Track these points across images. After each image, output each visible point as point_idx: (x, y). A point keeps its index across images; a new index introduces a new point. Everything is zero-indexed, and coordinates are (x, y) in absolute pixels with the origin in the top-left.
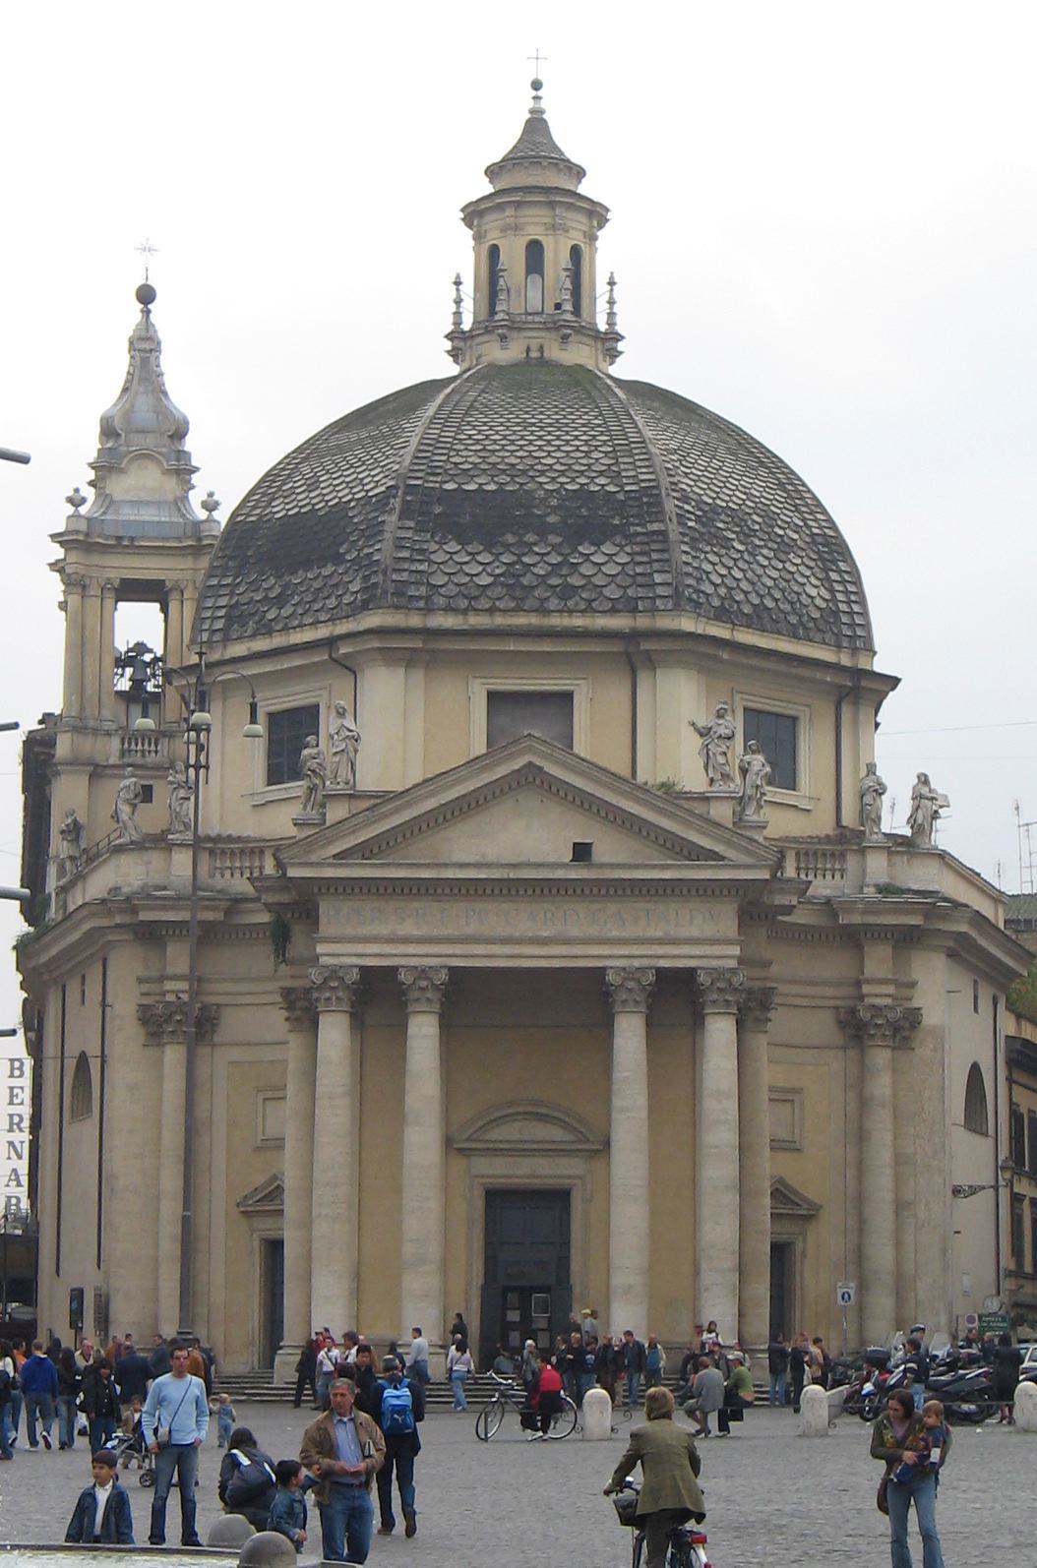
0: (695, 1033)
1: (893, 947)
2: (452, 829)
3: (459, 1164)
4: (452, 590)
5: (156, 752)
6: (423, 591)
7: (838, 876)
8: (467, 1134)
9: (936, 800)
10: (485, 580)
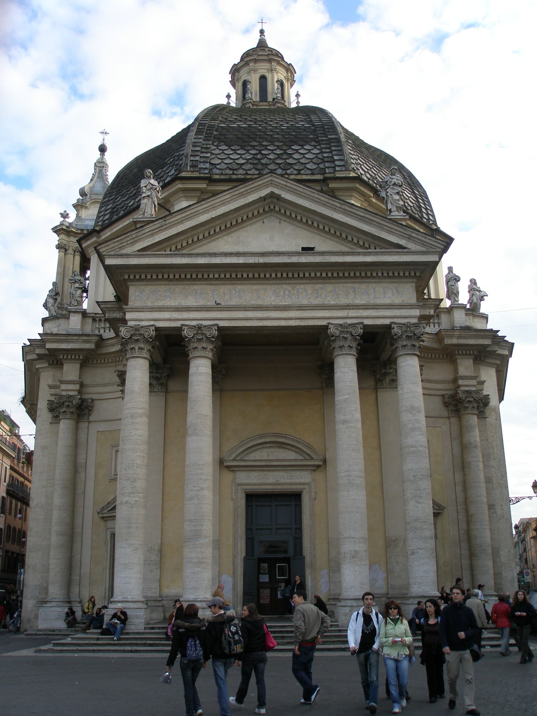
0: (377, 392)
1: (473, 360)
2: (221, 239)
3: (228, 476)
4: (223, 166)
6: (207, 165)
7: (437, 326)
8: (233, 456)
9: (481, 292)
10: (241, 161)
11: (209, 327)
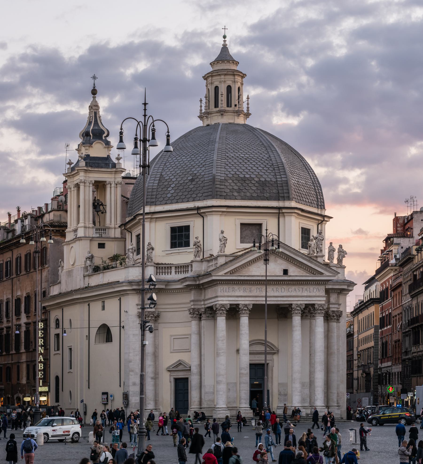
5: (105, 233)
11: (249, 304)
